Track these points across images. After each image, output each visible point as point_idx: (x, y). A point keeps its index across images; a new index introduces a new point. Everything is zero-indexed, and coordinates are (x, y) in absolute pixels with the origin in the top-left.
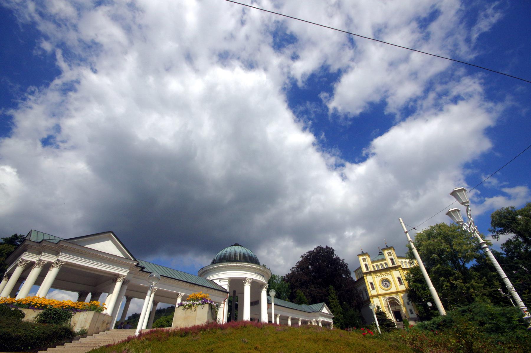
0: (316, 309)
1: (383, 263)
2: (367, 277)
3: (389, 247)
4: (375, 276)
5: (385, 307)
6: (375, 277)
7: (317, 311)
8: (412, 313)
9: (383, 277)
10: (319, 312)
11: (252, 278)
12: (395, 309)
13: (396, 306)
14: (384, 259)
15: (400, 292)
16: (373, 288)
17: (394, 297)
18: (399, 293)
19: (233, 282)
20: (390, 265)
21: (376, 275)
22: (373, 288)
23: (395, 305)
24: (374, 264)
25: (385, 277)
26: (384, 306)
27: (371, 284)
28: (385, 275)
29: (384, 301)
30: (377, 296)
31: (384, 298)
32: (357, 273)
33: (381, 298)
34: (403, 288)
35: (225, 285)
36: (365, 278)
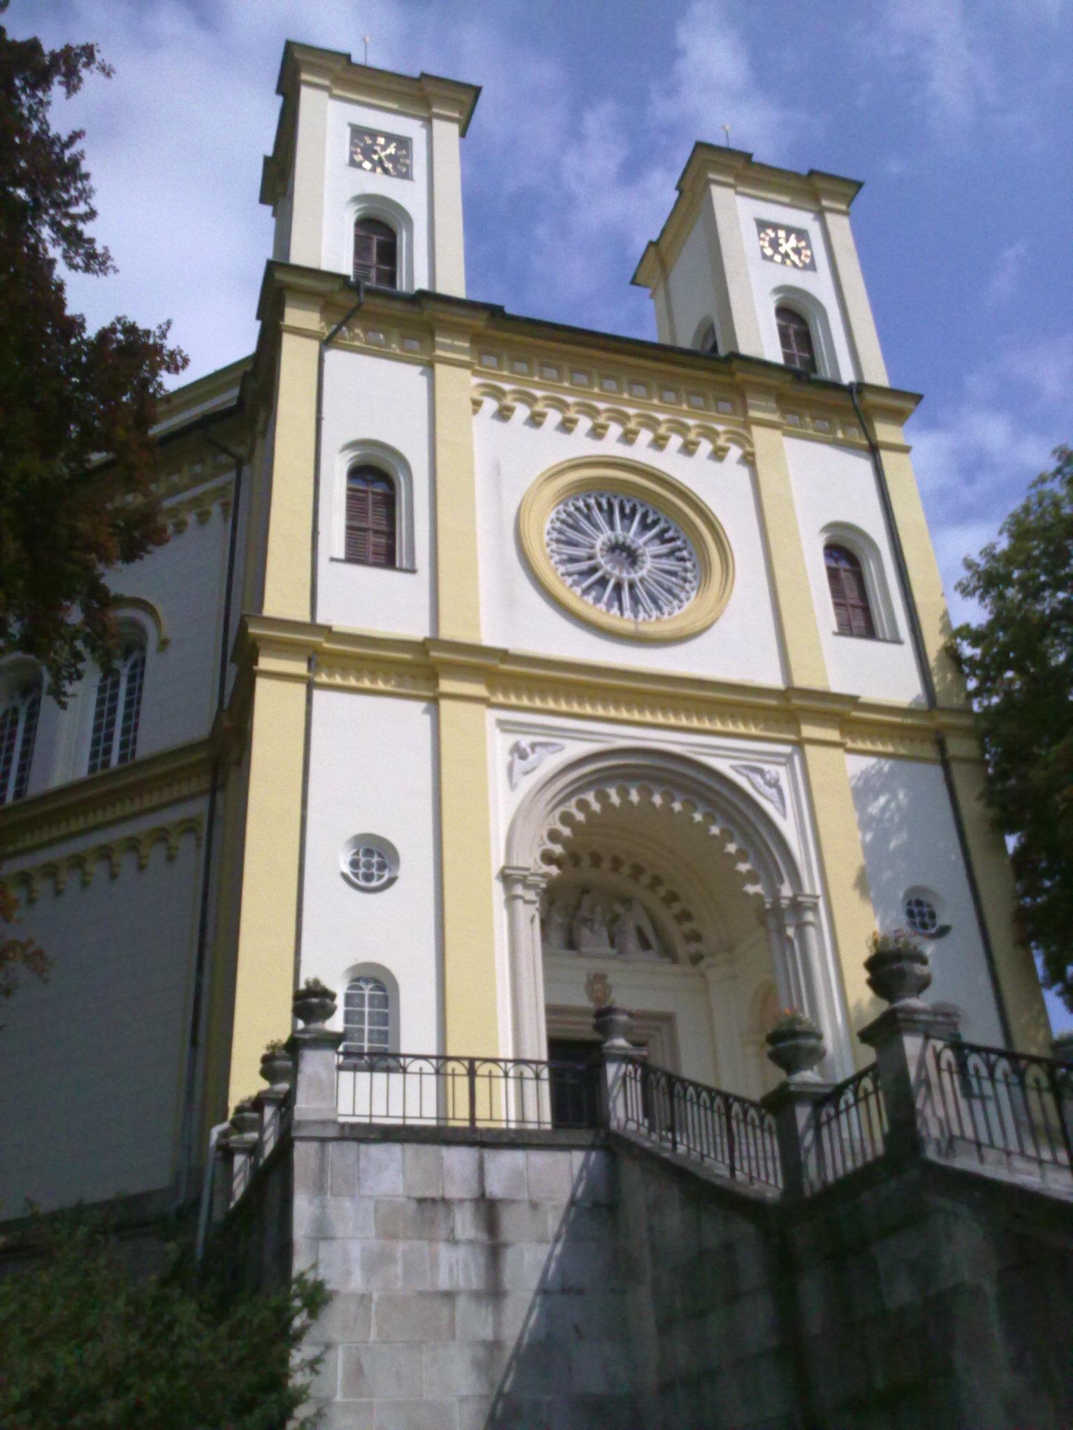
2: (332, 356)
5: (507, 878)
6: (490, 405)
17: (723, 766)
18: (808, 731)
26: (498, 860)
29: (527, 784)
31: (525, 741)
33: (492, 715)
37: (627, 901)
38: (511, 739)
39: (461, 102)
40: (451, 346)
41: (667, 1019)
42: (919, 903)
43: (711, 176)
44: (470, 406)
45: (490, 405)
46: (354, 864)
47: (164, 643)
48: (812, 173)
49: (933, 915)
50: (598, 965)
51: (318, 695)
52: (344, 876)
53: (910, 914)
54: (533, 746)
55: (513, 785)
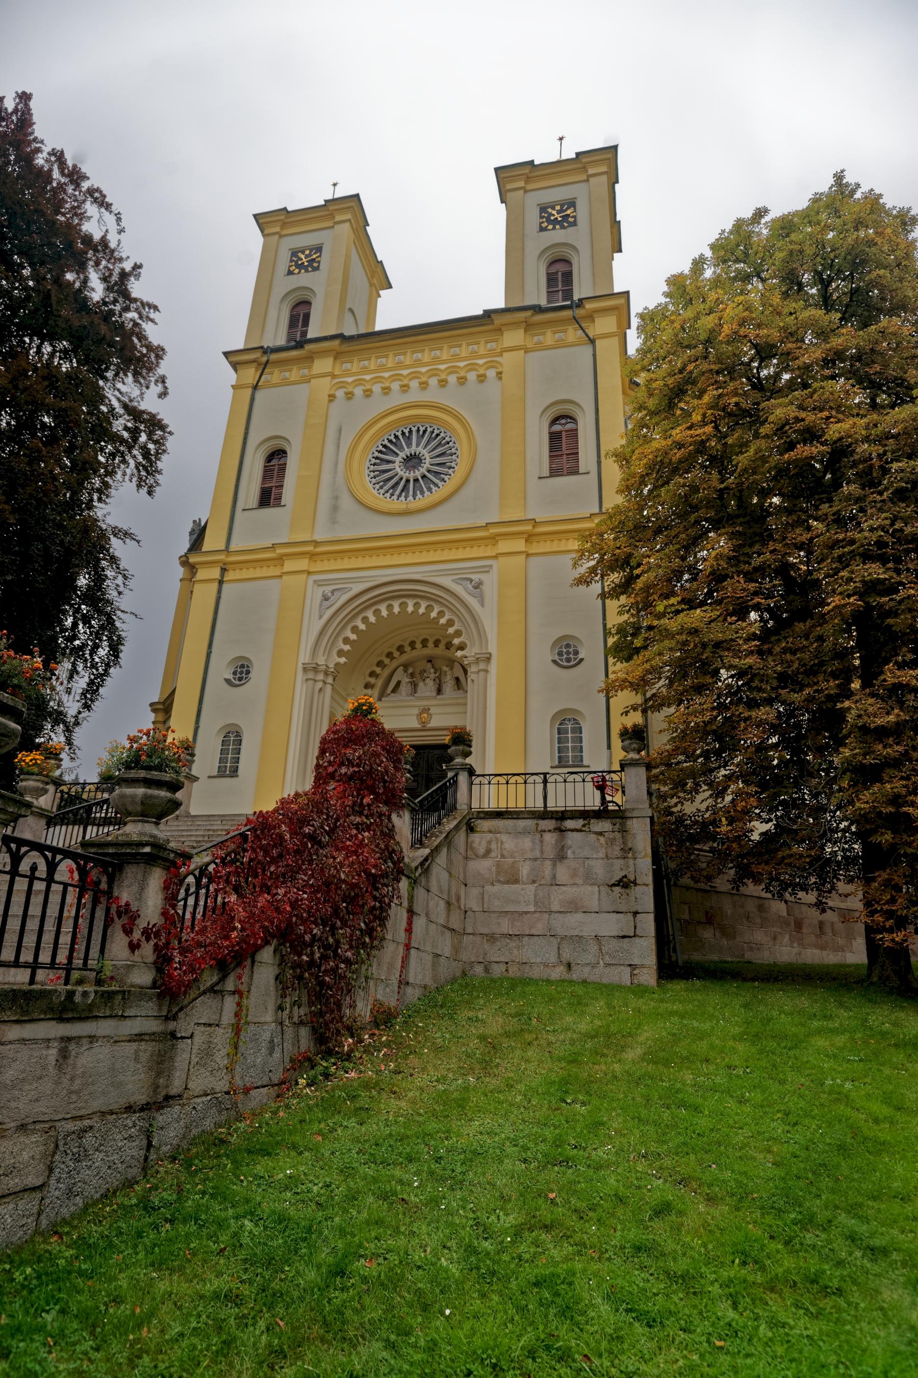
2: (259, 395)
4: (342, 385)
5: (305, 670)
12: (415, 724)
13: (439, 691)
17: (446, 582)
22: (268, 498)
28: (443, 383)
29: (329, 613)
37: (451, 662)
38: (321, 589)
39: (351, 207)
42: (568, 646)
43: (508, 186)
44: (327, 399)
45: (340, 394)
46: (235, 673)
48: (578, 154)
49: (576, 653)
51: (225, 586)
52: (228, 681)
53: (560, 654)
54: (333, 592)
55: (321, 617)
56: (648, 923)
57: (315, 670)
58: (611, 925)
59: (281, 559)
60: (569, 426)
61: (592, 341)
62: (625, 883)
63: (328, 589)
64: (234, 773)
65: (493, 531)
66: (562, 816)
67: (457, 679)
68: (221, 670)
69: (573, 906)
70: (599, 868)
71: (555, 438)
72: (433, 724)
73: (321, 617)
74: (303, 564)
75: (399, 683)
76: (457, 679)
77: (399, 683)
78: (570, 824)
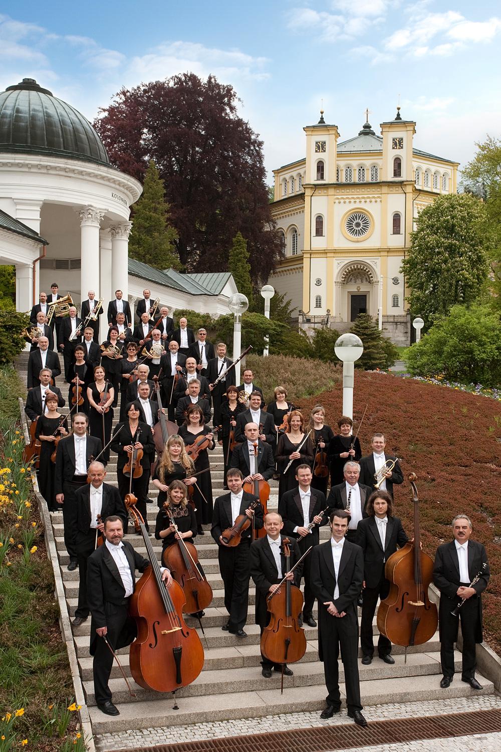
0: (210, 286)
1: (368, 162)
2: (312, 197)
3: (405, 123)
4: (338, 199)
5: (335, 283)
6: (337, 201)
7: (212, 292)
8: (395, 305)
9: (358, 205)
10: (219, 297)
11: (106, 210)
13: (362, 282)
14: (379, 153)
15: (389, 251)
16: (319, 232)
19: (49, 209)
20: (389, 176)
21: (339, 197)
22: (319, 232)
23: (360, 280)
24: (343, 163)
25: (363, 206)
26: (335, 280)
27: (319, 221)
29: (340, 268)
30: (325, 252)
31: (339, 262)
32: (282, 178)
34: (398, 241)
35: (32, 220)
36: (307, 199)
40: (331, 191)
41: (369, 292)
47: (299, 235)
50: (358, 285)
55: (337, 269)
56: (409, 339)
57: (338, 283)
58: (403, 339)
59: (326, 253)
60: (398, 218)
61: (405, 193)
62: (406, 333)
63: (339, 262)
64: (320, 307)
65: (380, 250)
66: (396, 323)
67: (366, 278)
68: (313, 282)
69: (398, 336)
70: (402, 331)
71: (394, 220)
72: (361, 290)
73: (337, 269)
74: (332, 255)
75: (351, 279)
76: (366, 278)
77: (351, 279)
78: (398, 324)
